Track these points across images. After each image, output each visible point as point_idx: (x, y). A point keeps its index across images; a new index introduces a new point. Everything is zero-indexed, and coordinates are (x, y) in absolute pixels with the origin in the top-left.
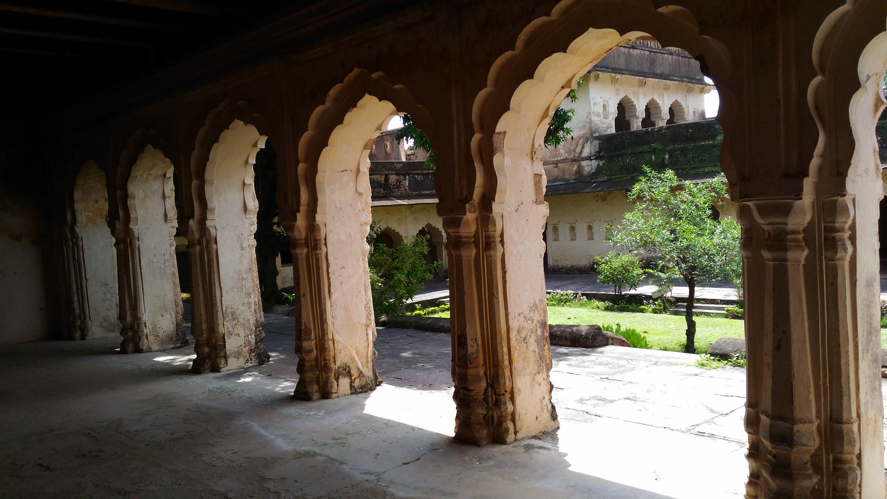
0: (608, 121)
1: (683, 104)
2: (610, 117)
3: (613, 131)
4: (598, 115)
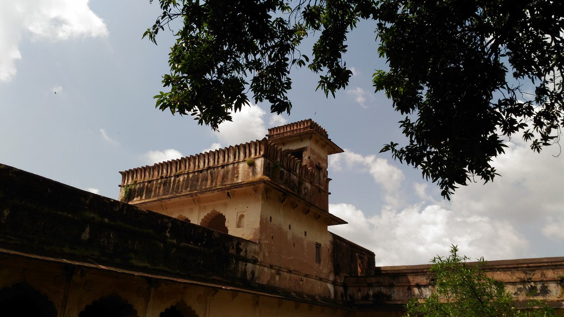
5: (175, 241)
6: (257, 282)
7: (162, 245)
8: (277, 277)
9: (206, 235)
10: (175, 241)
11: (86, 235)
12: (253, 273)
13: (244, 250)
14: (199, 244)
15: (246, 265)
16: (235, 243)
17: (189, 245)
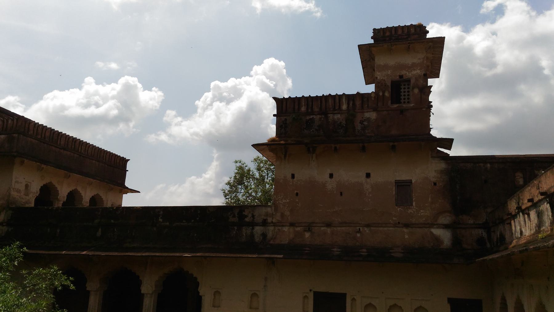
0: (27, 197)
1: (104, 197)
2: (31, 195)
3: (33, 205)
4: (19, 191)
5: (168, 224)
6: (272, 242)
7: (155, 229)
8: (307, 235)
9: (199, 212)
10: (168, 224)
11: (99, 233)
12: (264, 235)
13: (250, 215)
14: (193, 221)
15: (253, 229)
16: (236, 212)
17: (182, 224)
